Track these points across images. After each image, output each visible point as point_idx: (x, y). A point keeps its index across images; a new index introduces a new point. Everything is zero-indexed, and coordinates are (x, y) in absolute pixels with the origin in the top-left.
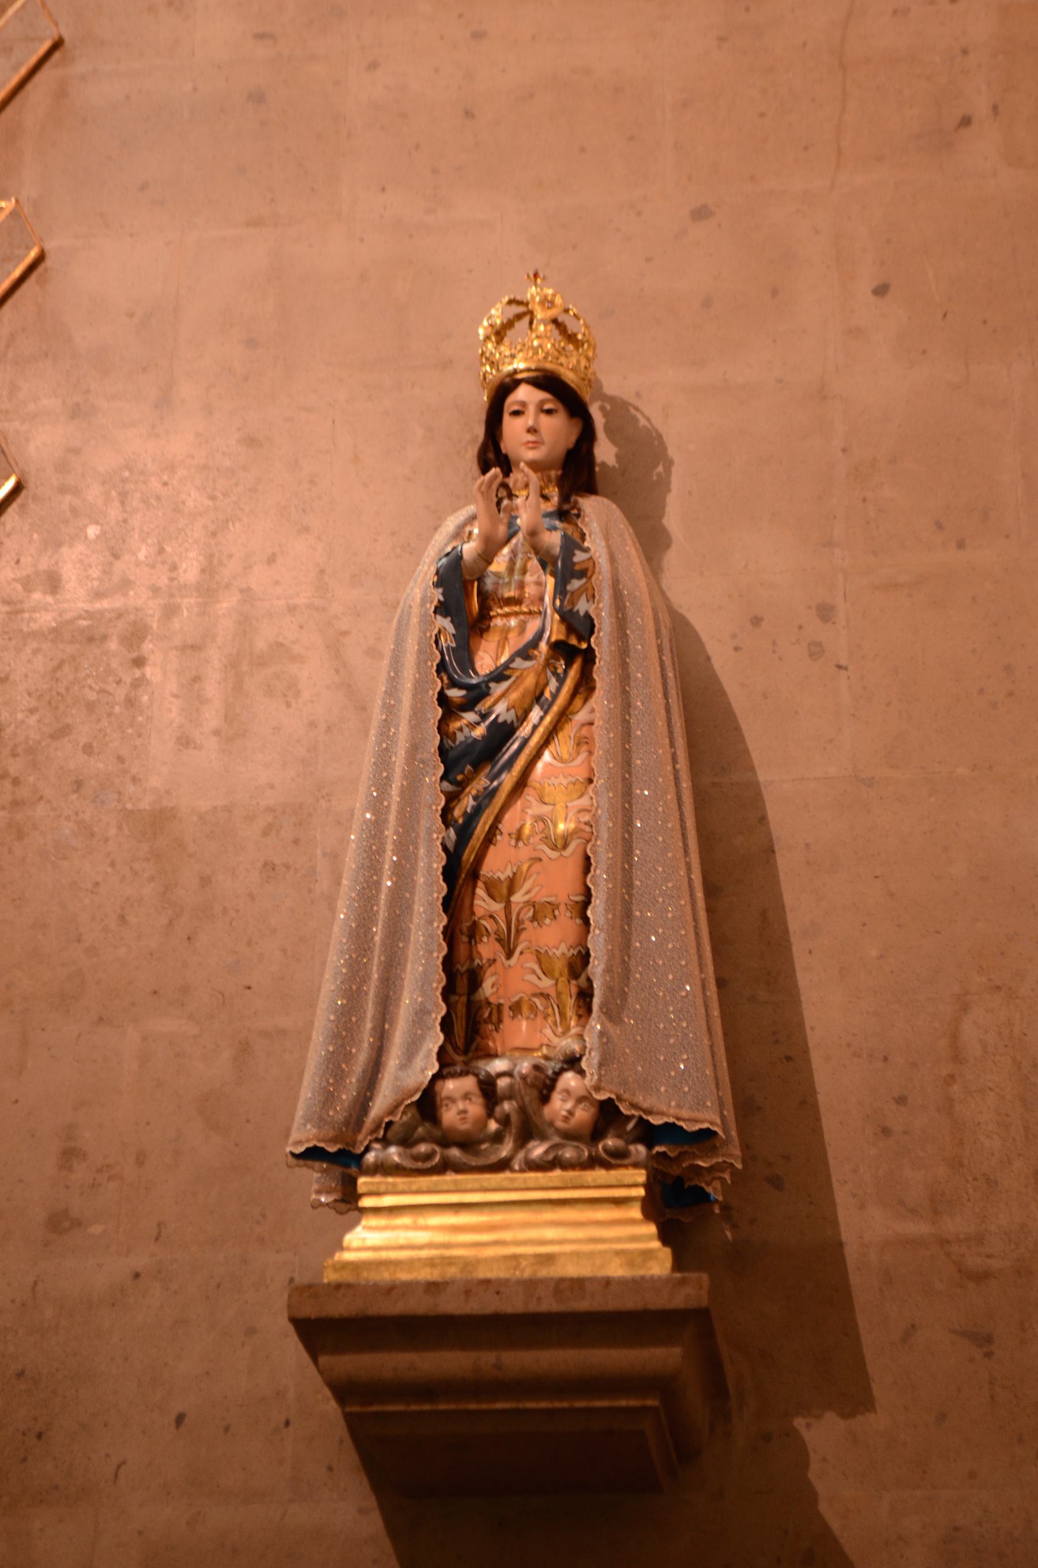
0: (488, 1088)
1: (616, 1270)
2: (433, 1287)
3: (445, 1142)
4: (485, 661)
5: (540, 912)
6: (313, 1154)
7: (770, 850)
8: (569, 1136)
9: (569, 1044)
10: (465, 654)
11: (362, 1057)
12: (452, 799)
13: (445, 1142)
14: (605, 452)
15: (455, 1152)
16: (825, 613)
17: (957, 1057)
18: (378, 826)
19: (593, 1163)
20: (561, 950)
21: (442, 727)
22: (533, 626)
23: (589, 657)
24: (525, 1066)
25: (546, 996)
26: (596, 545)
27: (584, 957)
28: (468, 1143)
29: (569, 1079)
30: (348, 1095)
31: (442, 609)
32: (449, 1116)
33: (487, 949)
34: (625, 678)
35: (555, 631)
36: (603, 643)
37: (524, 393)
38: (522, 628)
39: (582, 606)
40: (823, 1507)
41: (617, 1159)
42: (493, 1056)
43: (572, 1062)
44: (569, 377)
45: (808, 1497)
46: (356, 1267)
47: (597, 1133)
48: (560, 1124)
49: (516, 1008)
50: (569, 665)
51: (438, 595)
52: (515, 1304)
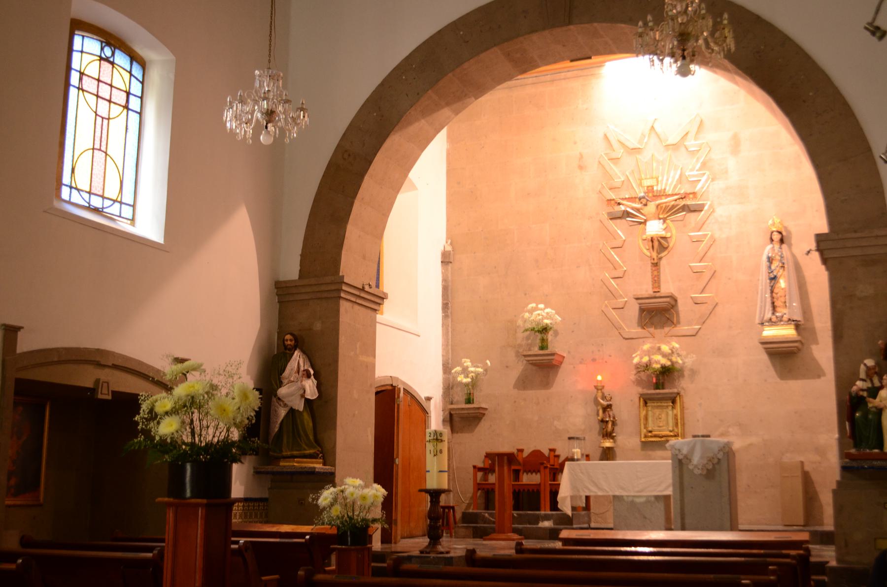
1: (791, 336)
2: (773, 339)
3: (772, 322)
4: (773, 267)
5: (781, 297)
6: (759, 324)
7: (805, 283)
8: (786, 322)
9: (785, 312)
10: (770, 267)
11: (763, 313)
12: (770, 283)
13: (772, 322)
14: (784, 233)
15: (773, 324)
18: (762, 289)
19: (788, 324)
20: (783, 301)
21: (769, 276)
23: (784, 267)
26: (784, 253)
27: (785, 302)
28: (775, 322)
29: (785, 316)
30: (762, 316)
32: (773, 320)
33: (775, 300)
34: (788, 268)
35: (781, 265)
36: (786, 266)
37: (775, 233)
39: (783, 261)
41: (791, 324)
42: (778, 312)
43: (785, 314)
46: (764, 336)
47: (788, 321)
49: (779, 307)
52: (781, 340)
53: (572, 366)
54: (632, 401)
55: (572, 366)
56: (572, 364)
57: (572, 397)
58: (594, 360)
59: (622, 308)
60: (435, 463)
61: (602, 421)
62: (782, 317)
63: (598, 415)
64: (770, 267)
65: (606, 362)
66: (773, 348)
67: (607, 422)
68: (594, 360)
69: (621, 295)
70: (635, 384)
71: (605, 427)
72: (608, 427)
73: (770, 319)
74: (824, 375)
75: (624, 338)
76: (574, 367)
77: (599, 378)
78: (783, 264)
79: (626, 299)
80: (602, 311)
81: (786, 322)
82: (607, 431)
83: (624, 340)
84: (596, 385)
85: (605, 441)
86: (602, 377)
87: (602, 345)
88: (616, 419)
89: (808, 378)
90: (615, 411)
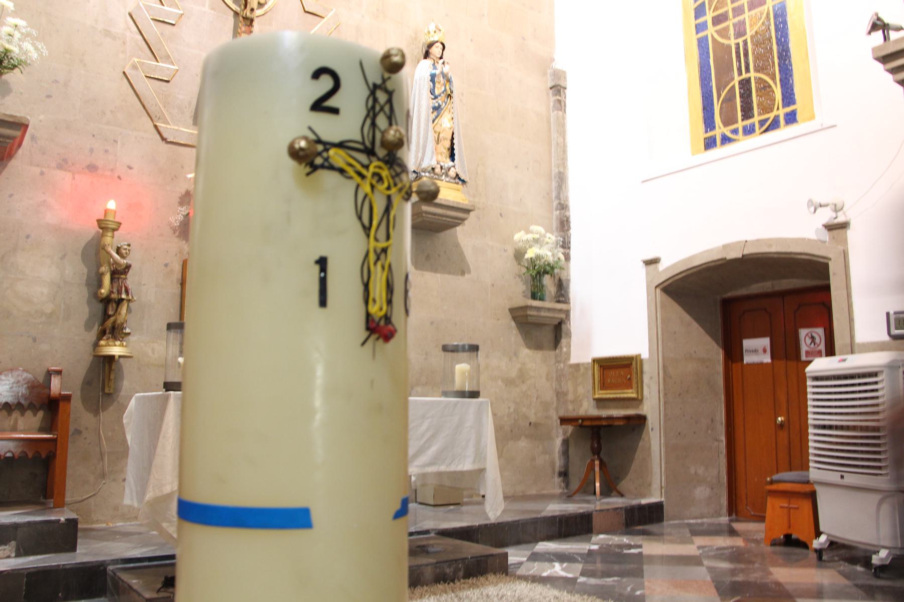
0: (441, 168)
4: (437, 92)
5: (445, 139)
8: (451, 178)
13: (435, 174)
16: (462, 94)
17: (477, 173)
19: (455, 183)
22: (443, 89)
24: (446, 166)
25: (444, 153)
28: (438, 175)
29: (452, 169)
30: (418, 163)
31: (431, 81)
38: (441, 88)
40: (459, 239)
41: (457, 183)
44: (443, 42)
45: (456, 237)
47: (455, 179)
48: (451, 176)
50: (448, 98)
51: (430, 78)
52: (451, 204)
53: (37, 170)
54: (166, 265)
55: (37, 170)
56: (38, 166)
57: (28, 237)
58: (92, 168)
59: (168, 82)
60: (318, 402)
61: (106, 301)
62: (449, 169)
63: (100, 285)
64: (432, 92)
65: (119, 177)
66: (435, 214)
67: (123, 300)
68: (92, 168)
69: (168, 57)
70: (177, 233)
71: (114, 315)
72: (120, 314)
73: (433, 169)
74: (469, 272)
75: (163, 139)
76: (42, 173)
77: (111, 205)
78: (452, 92)
79: (177, 68)
80: (124, 73)
81: (451, 178)
82: (114, 322)
83: (163, 144)
84: (102, 217)
85: (110, 343)
86: (117, 205)
87: (115, 141)
88: (135, 299)
89: (450, 273)
90: (131, 280)
